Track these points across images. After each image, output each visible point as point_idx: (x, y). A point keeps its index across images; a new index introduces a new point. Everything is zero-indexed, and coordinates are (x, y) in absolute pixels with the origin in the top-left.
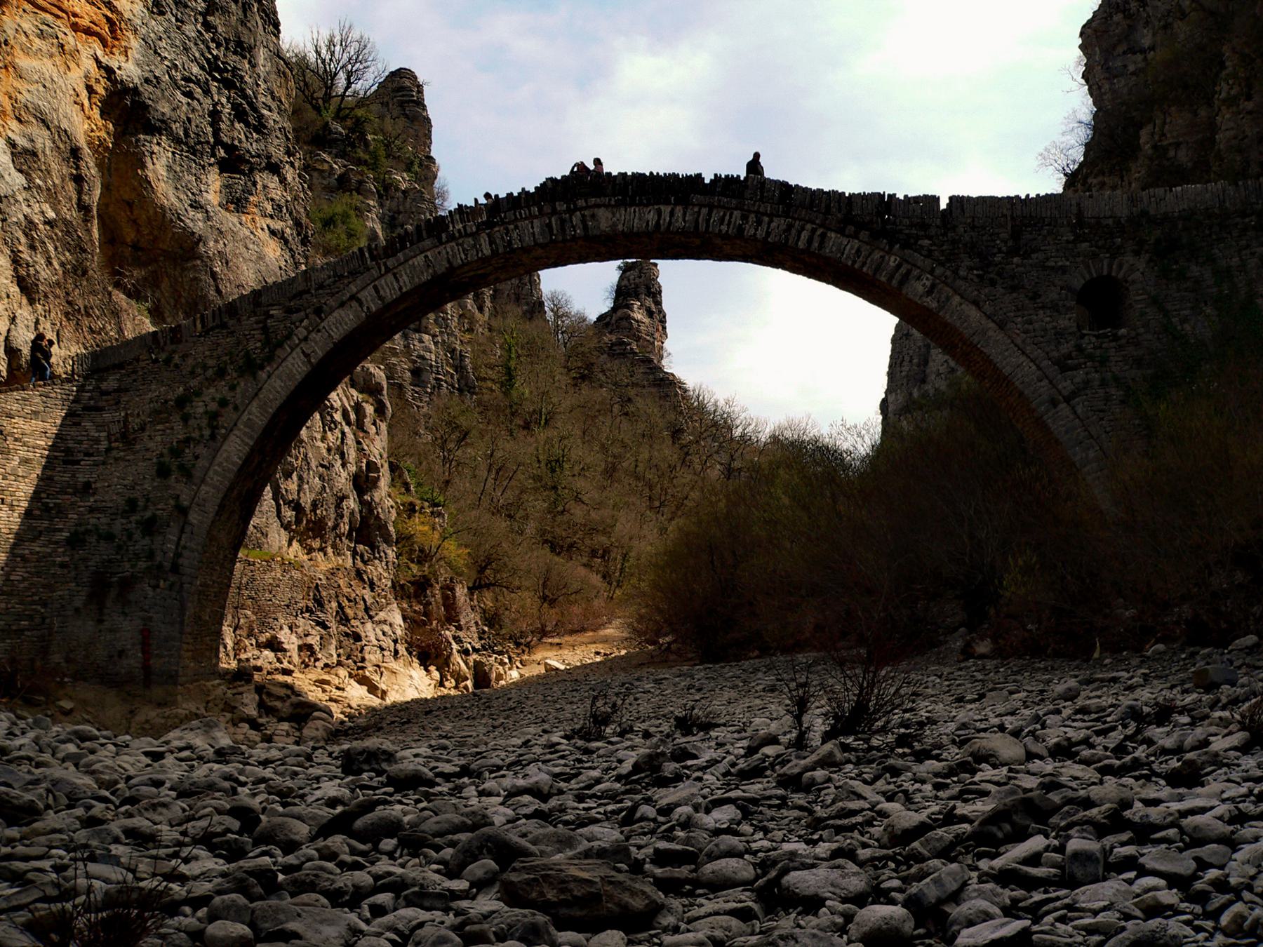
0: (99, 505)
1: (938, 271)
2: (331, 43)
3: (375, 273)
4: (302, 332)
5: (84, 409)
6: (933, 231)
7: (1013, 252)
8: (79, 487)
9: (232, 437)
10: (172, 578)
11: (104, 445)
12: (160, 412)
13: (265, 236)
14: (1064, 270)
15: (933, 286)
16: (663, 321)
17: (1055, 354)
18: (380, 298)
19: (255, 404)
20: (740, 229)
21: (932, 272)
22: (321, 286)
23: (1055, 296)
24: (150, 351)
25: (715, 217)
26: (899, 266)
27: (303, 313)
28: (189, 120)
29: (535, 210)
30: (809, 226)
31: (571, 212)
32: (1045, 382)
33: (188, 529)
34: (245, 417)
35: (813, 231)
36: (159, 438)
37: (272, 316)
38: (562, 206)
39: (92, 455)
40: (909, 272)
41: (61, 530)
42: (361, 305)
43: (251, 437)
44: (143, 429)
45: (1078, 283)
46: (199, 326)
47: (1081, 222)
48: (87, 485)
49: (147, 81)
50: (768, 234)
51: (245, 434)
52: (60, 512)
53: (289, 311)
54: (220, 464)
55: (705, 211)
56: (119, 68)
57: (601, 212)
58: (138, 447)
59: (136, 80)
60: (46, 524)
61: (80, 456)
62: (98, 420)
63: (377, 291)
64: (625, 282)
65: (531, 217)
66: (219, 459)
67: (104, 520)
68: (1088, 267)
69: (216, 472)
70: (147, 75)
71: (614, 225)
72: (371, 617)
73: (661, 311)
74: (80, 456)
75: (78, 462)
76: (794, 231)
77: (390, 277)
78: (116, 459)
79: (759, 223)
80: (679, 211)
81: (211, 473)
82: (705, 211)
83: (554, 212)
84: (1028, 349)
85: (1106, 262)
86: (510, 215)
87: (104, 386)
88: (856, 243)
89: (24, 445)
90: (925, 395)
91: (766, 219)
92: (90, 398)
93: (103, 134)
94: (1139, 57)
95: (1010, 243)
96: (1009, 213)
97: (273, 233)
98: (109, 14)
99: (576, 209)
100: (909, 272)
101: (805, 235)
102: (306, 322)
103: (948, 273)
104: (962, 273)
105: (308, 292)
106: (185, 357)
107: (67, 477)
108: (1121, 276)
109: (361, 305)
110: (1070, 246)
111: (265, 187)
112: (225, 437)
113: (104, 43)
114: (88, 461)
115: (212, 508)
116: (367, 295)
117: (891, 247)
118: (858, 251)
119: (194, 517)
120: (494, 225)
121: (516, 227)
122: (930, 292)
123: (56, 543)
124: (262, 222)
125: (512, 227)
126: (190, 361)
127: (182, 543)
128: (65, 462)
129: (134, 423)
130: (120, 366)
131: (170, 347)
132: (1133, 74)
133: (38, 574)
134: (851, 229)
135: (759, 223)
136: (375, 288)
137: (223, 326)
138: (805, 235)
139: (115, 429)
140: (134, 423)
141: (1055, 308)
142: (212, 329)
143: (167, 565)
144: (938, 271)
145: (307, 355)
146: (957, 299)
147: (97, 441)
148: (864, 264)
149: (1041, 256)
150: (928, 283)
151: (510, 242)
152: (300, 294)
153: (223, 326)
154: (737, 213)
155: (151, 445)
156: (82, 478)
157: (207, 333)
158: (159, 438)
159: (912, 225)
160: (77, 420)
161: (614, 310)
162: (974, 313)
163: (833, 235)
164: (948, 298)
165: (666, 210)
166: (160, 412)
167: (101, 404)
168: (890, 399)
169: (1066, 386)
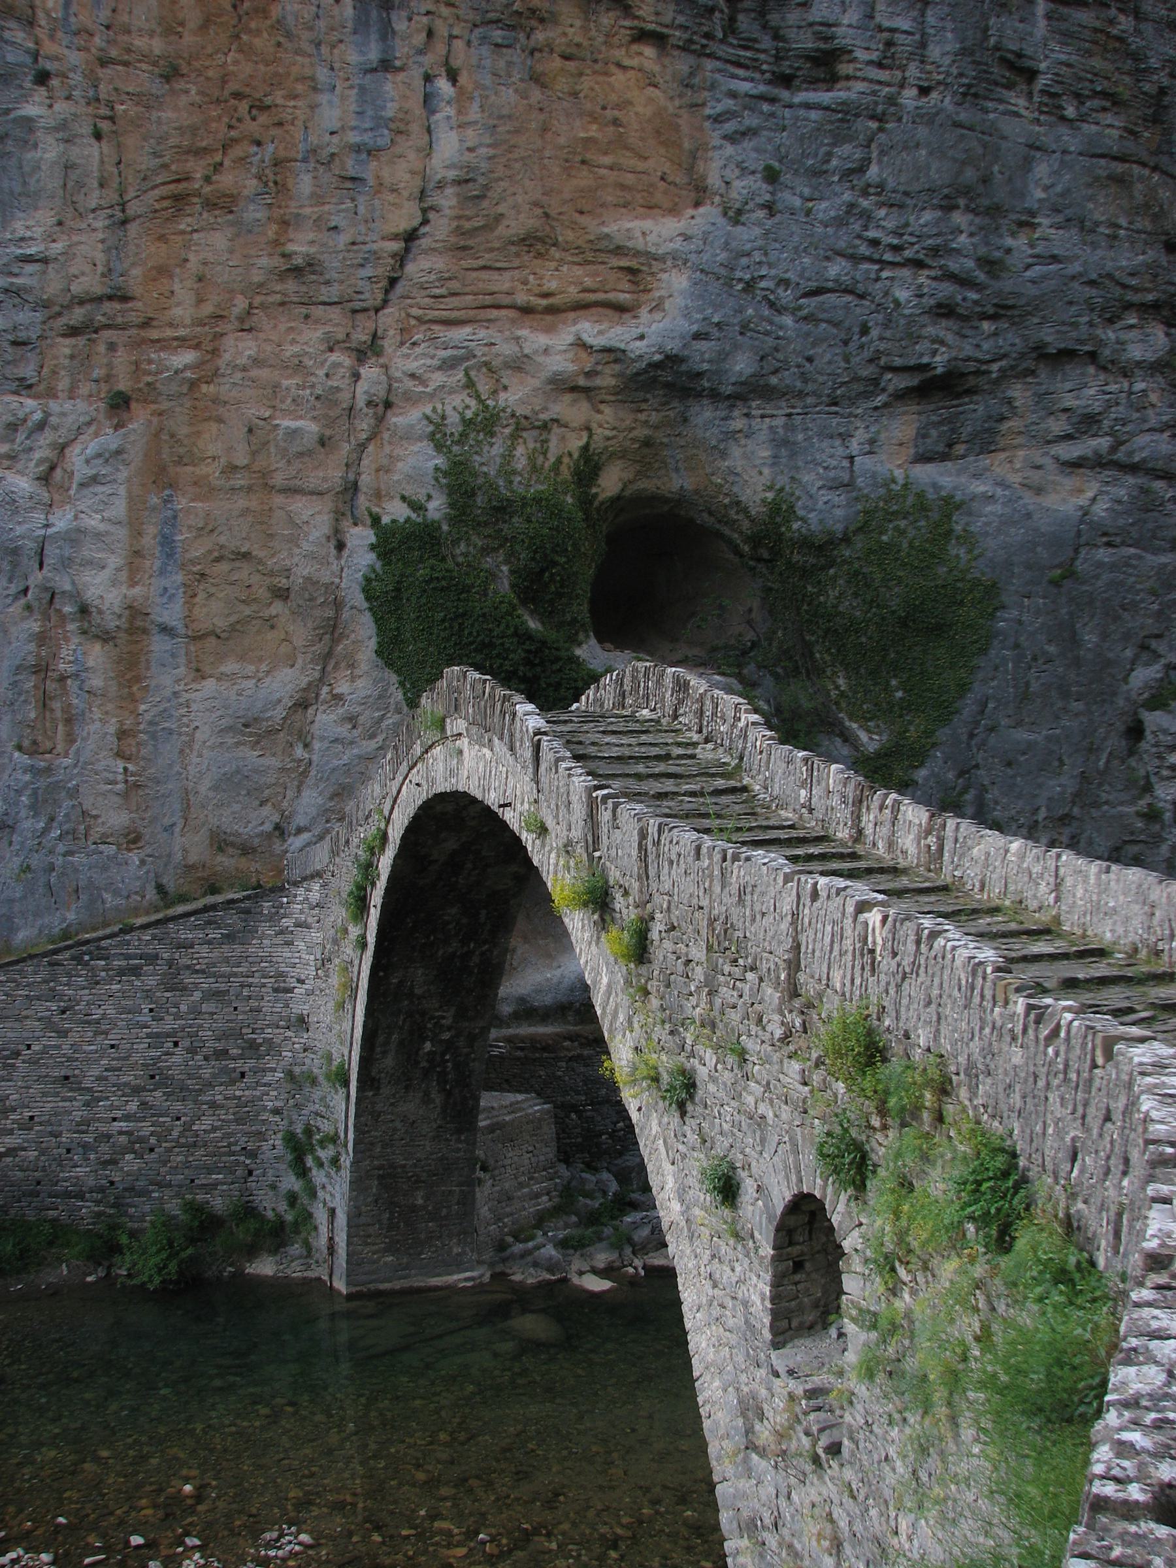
5: (298, 925)
28: (810, 360)
41: (274, 1070)
49: (697, 336)
56: (642, 337)
59: (673, 346)
60: (252, 1063)
70: (695, 328)
89: (214, 975)
92: (302, 912)
93: (641, 432)
97: (1075, 465)
98: (625, 263)
111: (1040, 397)
128: (276, 990)
133: (238, 1121)
156: (297, 1009)
160: (289, 937)
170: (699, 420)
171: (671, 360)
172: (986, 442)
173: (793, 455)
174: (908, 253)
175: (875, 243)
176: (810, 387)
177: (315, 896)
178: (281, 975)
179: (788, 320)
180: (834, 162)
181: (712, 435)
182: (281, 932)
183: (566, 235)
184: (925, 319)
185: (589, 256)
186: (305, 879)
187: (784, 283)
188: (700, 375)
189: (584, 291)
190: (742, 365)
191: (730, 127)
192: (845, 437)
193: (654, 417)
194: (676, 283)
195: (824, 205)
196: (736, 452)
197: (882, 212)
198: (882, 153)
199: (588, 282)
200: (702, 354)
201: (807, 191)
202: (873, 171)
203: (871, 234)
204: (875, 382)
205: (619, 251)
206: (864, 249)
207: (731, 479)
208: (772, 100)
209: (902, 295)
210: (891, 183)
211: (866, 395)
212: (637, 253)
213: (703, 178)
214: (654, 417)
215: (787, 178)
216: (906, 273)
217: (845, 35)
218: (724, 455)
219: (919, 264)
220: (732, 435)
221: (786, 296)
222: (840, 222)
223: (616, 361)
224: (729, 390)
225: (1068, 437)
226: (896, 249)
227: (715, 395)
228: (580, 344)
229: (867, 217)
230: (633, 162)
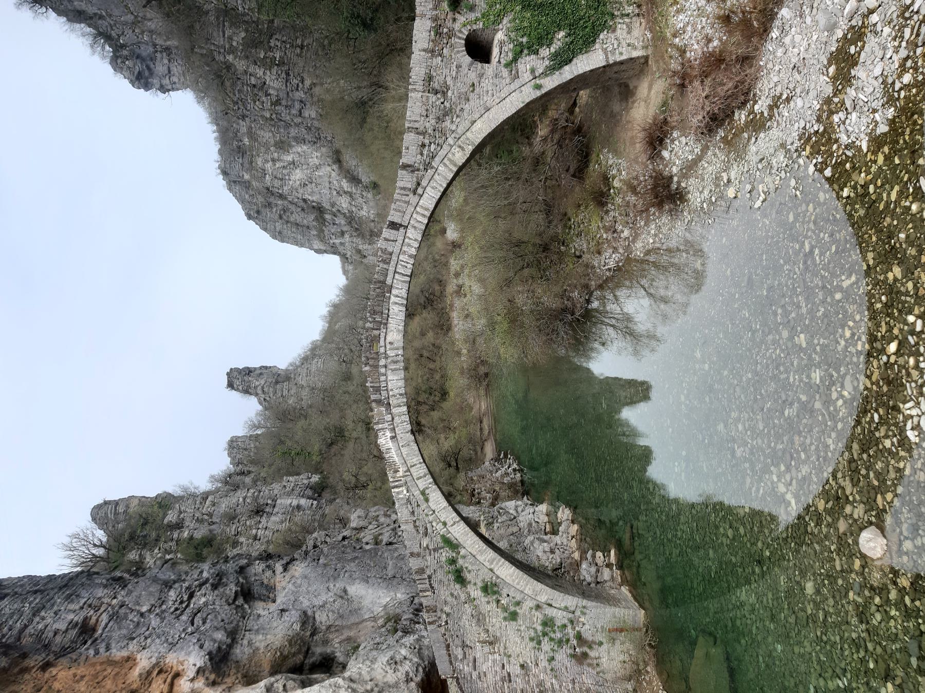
0: (533, 660)
1: (452, 143)
2: (69, 557)
3: (409, 479)
4: (440, 526)
5: (475, 670)
6: (427, 141)
7: (444, 94)
8: (523, 672)
9: (498, 573)
10: (578, 613)
11: (497, 656)
12: (479, 619)
13: (288, 575)
14: (459, 67)
15: (460, 147)
16: (266, 368)
17: (508, 81)
18: (425, 476)
19: (478, 557)
20: (410, 256)
21: (451, 146)
22: (413, 513)
23: (474, 74)
24: (440, 626)
25: (400, 269)
26: (445, 165)
27: (428, 525)
28: (223, 621)
29: (383, 378)
30: (414, 216)
31: (386, 358)
32: (523, 88)
33: (550, 602)
34: (487, 564)
35: (417, 213)
36: (494, 620)
37: (427, 546)
38: (382, 362)
39: (503, 665)
40: (449, 160)
41: (552, 684)
42: (427, 488)
43: (499, 560)
44: (488, 631)
45: (468, 59)
46: (428, 593)
47: (433, 51)
48: (522, 666)
49: (201, 647)
50: (416, 240)
51: (497, 564)
52: (541, 685)
53: (426, 534)
54: (513, 581)
55: (397, 276)
56: (195, 665)
57: (389, 339)
58: (498, 635)
59: (202, 653)
61: (505, 672)
62: (482, 660)
63: (421, 478)
64: (240, 388)
65: (386, 381)
66: (511, 583)
67: (542, 657)
68: (458, 52)
69: (518, 584)
70: (197, 647)
71: (398, 331)
72: (515, 518)
73: (261, 368)
74: (505, 672)
75: (509, 674)
76: (416, 225)
77: (412, 470)
78: (505, 648)
79: (409, 245)
80: (394, 292)
81: (518, 587)
82: (397, 276)
83: (386, 366)
84: (503, 96)
85: (457, 40)
86: (384, 393)
87: (460, 657)
88: (428, 189)
90: (315, 227)
91: (407, 240)
93: (239, 675)
94: (158, 55)
95: (439, 96)
96: (421, 94)
98: (155, 672)
99: (385, 353)
100: (449, 160)
101: (420, 218)
102: (434, 524)
103: (453, 136)
104: (454, 128)
105: (415, 522)
106: (446, 603)
107: (519, 680)
108: (467, 33)
109: (427, 488)
110: (445, 59)
112: (498, 577)
113: (177, 675)
114: (507, 666)
115: (539, 586)
116: (422, 484)
117: (432, 168)
118: (433, 188)
119: (543, 598)
120: (389, 404)
121: (392, 390)
122: (463, 149)
123: (560, 687)
124: (279, 577)
125: (391, 393)
126: (449, 599)
127: (558, 606)
128: (510, 681)
129: (484, 636)
130: (448, 646)
131: (439, 613)
132: (169, 61)
134: (420, 191)
135: (409, 245)
136: (418, 479)
137: (430, 577)
138: (420, 218)
139: (487, 649)
140: (484, 636)
141: (481, 76)
142: (430, 585)
143: (571, 615)
144: (451, 141)
145: (454, 523)
146: (469, 134)
147: (494, 661)
148: (441, 185)
149: (449, 79)
150: (458, 149)
151: (401, 395)
152: (415, 527)
153: (430, 577)
154: (401, 257)
155: (498, 625)
156: (518, 670)
157: (432, 588)
158: (494, 620)
159: (422, 154)
160: (482, 675)
161: (257, 395)
162: (478, 125)
163: (421, 201)
164: (468, 139)
165: (393, 299)
166: (479, 619)
167: (471, 659)
168: (316, 247)
169: (527, 76)
170: (239, 656)
171: (210, 654)
172: (271, 589)
173: (263, 629)
174: (186, 598)
175: (176, 609)
176: (235, 623)
177: (459, 652)
178: (503, 680)
179: (202, 628)
180: (135, 619)
181: (247, 650)
182: (480, 678)
183: (134, 686)
184: (216, 592)
185: (147, 682)
186: (451, 663)
187: (184, 630)
188: (219, 648)
189: (165, 682)
190: (220, 636)
191: (102, 650)
192: (259, 616)
193: (233, 671)
194: (172, 659)
195: (153, 622)
196: (257, 644)
197: (164, 607)
198: (139, 604)
199: (160, 681)
200: (208, 646)
201: (145, 629)
202: (144, 609)
203: (172, 609)
204: (238, 606)
205: (149, 673)
206: (178, 612)
207: (269, 648)
208: (96, 639)
209: (203, 600)
210: (153, 602)
211: (243, 609)
212: (153, 667)
213: (123, 657)
214: (233, 671)
215: (134, 635)
216: (193, 600)
217: (79, 618)
218: (258, 649)
219: (191, 596)
220: (250, 644)
221: (190, 630)
222: (163, 619)
223: (204, 671)
224: (229, 641)
225: (274, 572)
226: (182, 602)
227: (230, 646)
228: (192, 680)
229: (163, 612)
230: (105, 673)
